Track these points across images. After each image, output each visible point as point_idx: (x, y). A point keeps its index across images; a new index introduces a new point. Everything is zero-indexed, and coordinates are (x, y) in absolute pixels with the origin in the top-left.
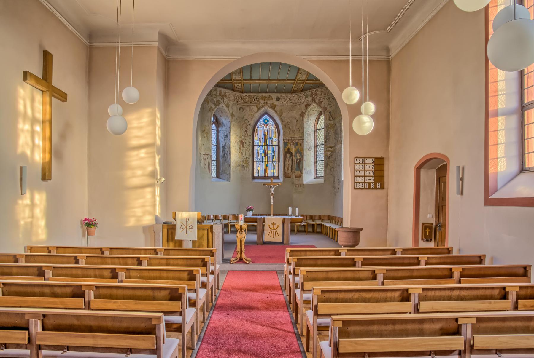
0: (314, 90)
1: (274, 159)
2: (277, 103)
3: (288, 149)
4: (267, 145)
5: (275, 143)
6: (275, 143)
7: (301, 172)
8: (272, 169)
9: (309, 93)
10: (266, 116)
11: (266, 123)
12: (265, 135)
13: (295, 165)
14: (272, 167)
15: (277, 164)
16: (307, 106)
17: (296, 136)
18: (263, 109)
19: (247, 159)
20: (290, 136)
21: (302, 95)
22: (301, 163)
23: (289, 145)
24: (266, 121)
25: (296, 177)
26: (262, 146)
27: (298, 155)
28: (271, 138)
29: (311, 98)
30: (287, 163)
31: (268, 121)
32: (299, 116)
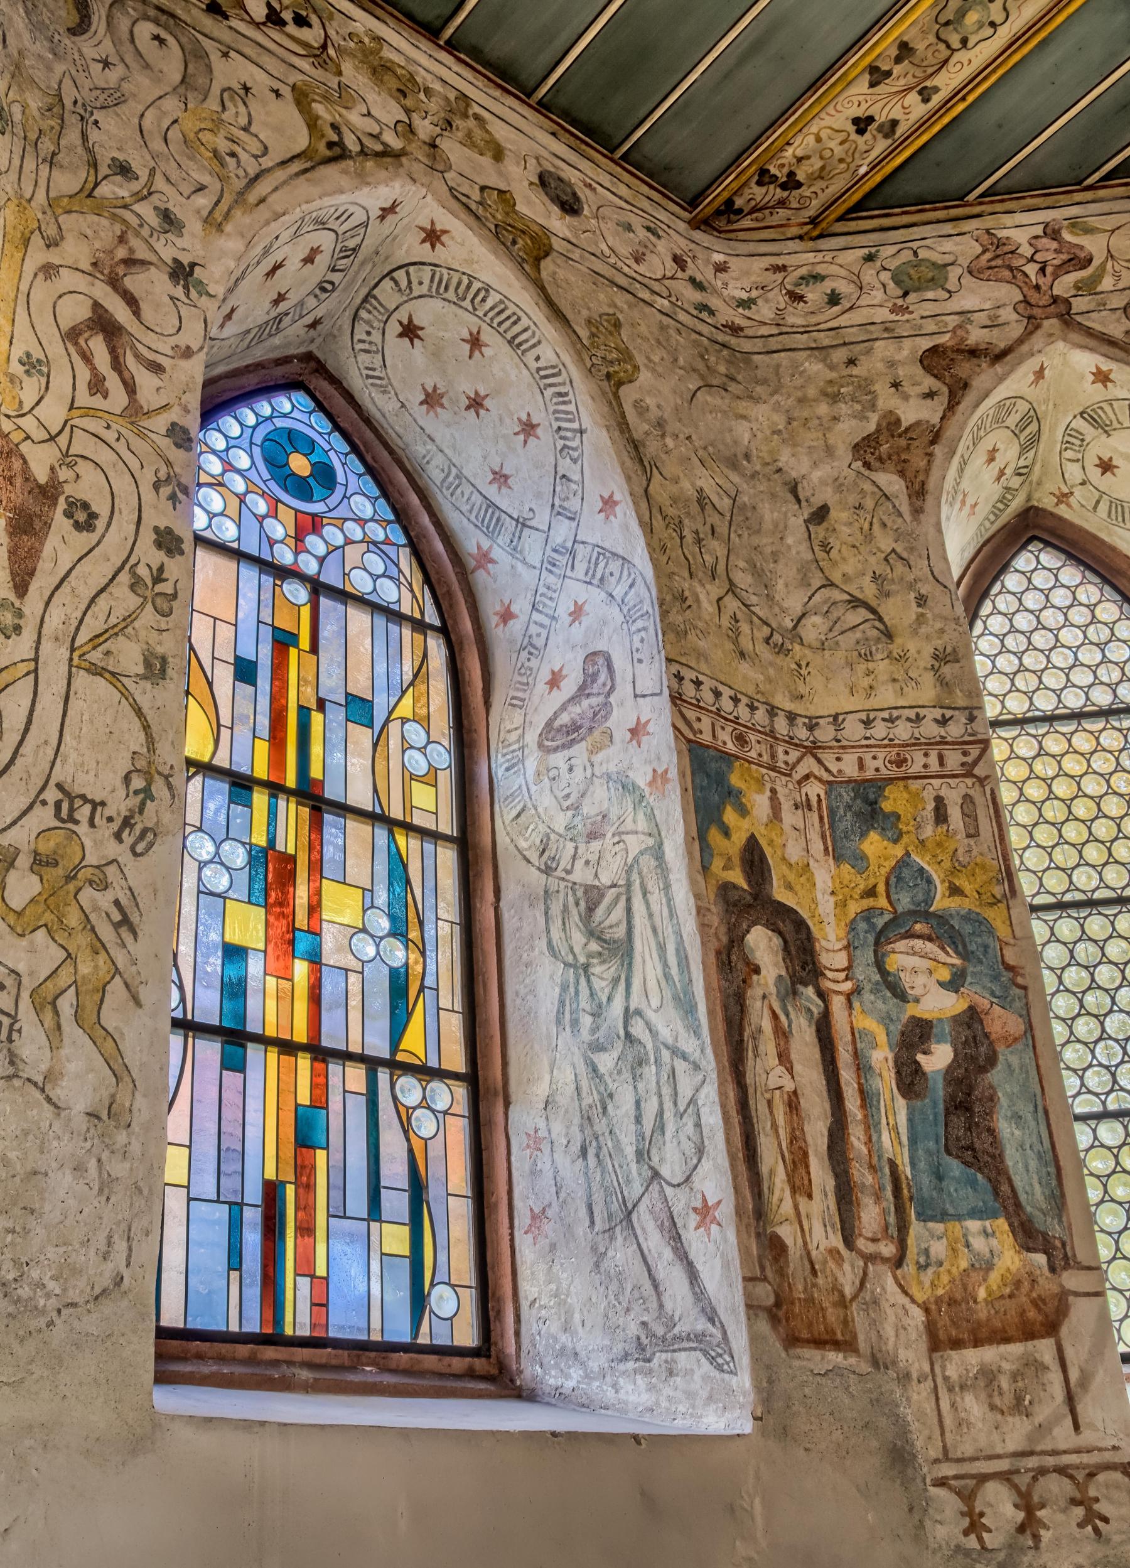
0: (1020, 227)
1: (413, 1042)
2: (558, 224)
3: (754, 859)
4: (314, 799)
5: (422, 796)
6: (422, 796)
7: (1028, 1235)
8: (396, 1203)
9: (953, 245)
10: (290, 409)
11: (301, 488)
12: (283, 642)
13: (893, 1129)
14: (394, 1171)
15: (458, 1131)
16: (954, 367)
17: (829, 696)
18: (360, 197)
19: (97, 844)
20: (747, 676)
21: (839, 261)
22: (1004, 1082)
23: (760, 803)
24: (299, 464)
25: (938, 1342)
26: (241, 785)
27: (919, 965)
28: (359, 708)
29: (1009, 294)
30: (766, 1070)
31: (325, 475)
32: (843, 463)
